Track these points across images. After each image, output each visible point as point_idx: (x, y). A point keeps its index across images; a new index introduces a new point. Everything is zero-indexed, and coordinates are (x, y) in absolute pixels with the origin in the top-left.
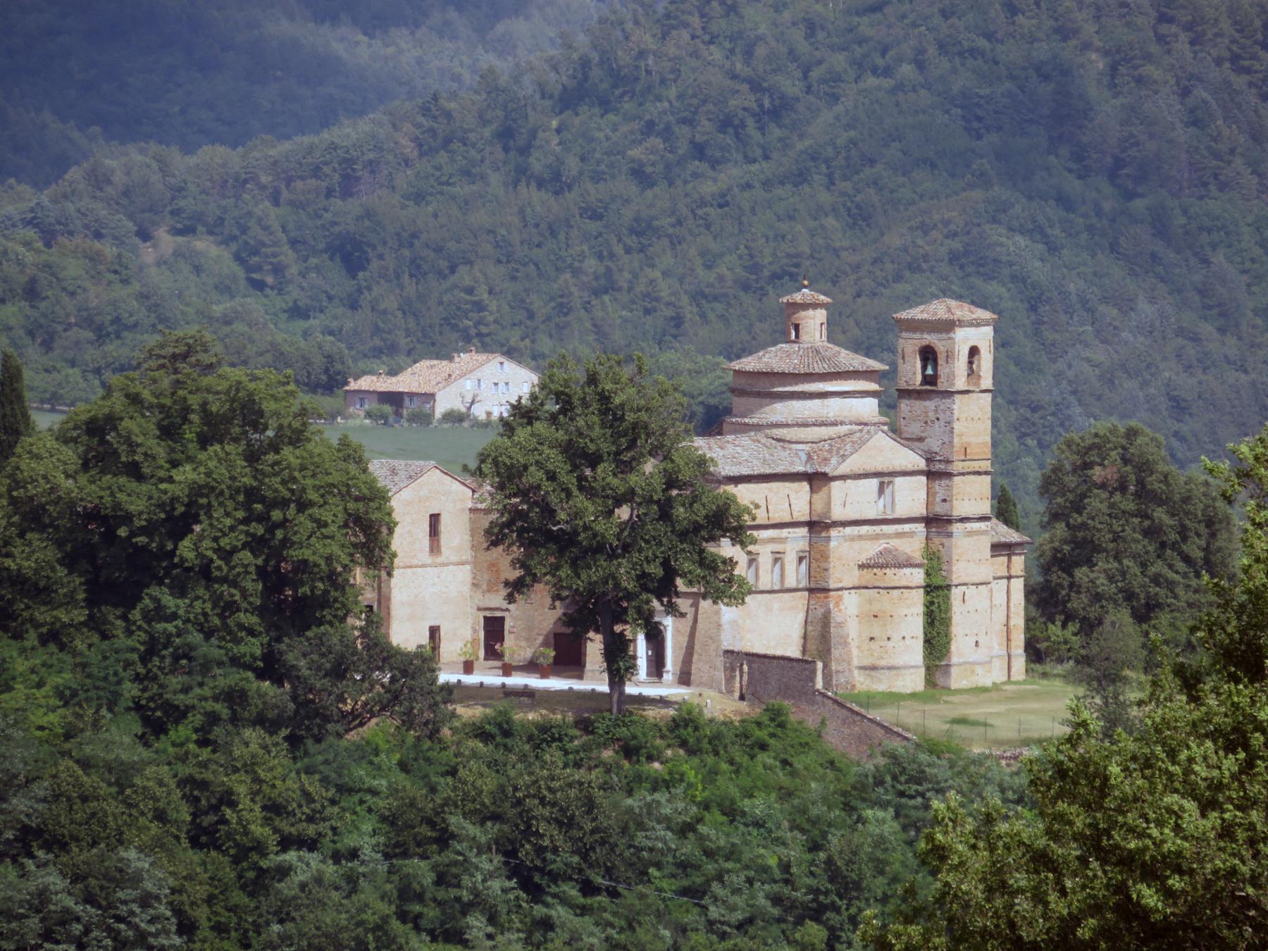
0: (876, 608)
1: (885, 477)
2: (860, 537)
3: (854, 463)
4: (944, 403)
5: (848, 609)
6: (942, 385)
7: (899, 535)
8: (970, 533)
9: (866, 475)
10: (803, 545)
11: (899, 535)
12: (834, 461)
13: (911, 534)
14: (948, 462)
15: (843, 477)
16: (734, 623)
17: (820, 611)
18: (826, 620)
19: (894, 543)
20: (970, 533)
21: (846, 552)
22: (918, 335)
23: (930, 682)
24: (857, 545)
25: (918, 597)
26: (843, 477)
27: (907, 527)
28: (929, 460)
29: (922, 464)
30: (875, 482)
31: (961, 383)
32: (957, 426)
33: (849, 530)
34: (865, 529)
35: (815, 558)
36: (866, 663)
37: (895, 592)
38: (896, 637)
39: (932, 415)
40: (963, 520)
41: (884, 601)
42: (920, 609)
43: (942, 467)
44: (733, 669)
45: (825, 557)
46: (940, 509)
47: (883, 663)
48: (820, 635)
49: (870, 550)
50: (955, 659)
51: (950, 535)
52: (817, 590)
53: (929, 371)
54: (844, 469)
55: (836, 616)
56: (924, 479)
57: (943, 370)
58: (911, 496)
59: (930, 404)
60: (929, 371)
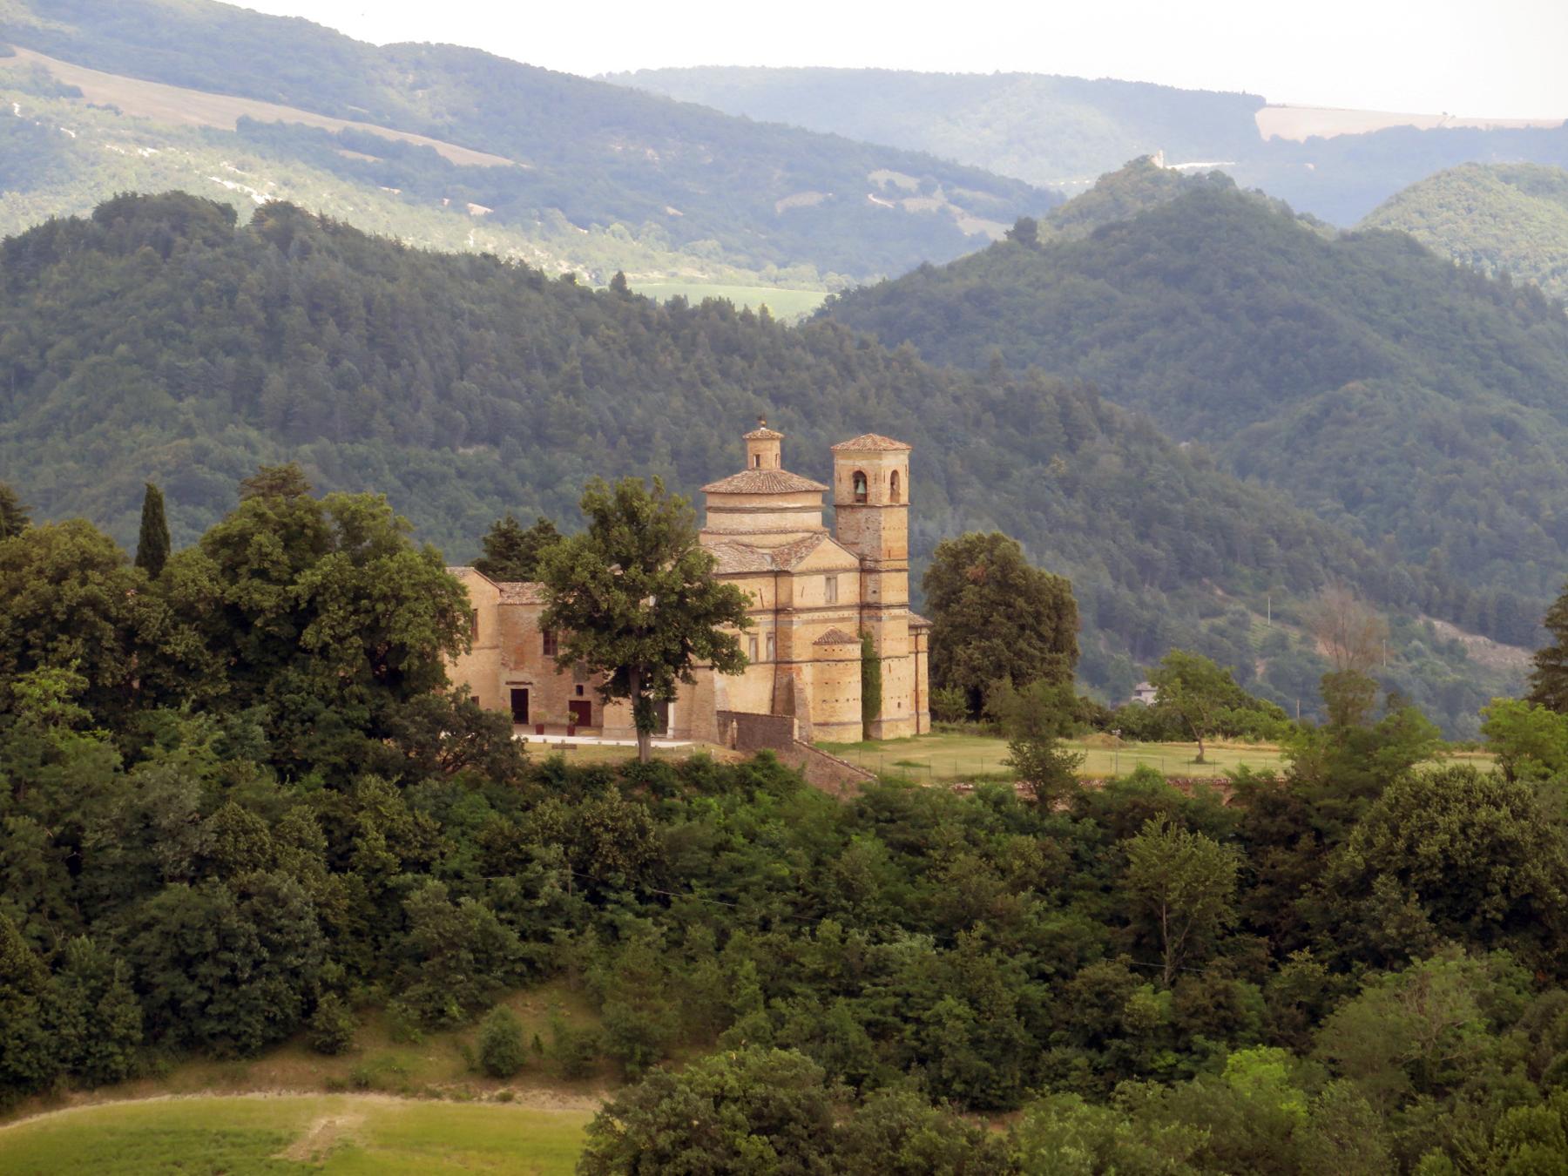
0: (827, 676)
1: (830, 574)
2: (813, 621)
3: (811, 561)
4: (874, 513)
5: (806, 677)
6: (871, 500)
7: (842, 620)
8: (895, 618)
9: (818, 572)
10: (770, 628)
11: (842, 620)
12: (794, 561)
13: (849, 619)
14: (877, 561)
15: (802, 574)
16: (724, 691)
17: (785, 680)
18: (790, 687)
19: (839, 626)
20: (895, 618)
21: (804, 634)
22: (850, 462)
23: (866, 736)
24: (811, 628)
25: (858, 666)
26: (802, 574)
27: (846, 613)
28: (862, 560)
29: (855, 562)
30: (823, 578)
31: (886, 500)
32: (884, 534)
33: (805, 616)
34: (816, 615)
35: (779, 637)
36: (820, 720)
37: (841, 665)
38: (842, 699)
39: (863, 526)
40: (889, 607)
41: (834, 671)
42: (858, 677)
43: (872, 565)
44: (725, 725)
45: (789, 637)
46: (870, 599)
47: (833, 720)
48: (786, 698)
49: (821, 631)
50: (884, 717)
51: (879, 619)
52: (782, 663)
53: (861, 490)
54: (802, 566)
55: (798, 683)
56: (857, 575)
57: (872, 489)
58: (848, 589)
59: (862, 515)
60: (861, 490)
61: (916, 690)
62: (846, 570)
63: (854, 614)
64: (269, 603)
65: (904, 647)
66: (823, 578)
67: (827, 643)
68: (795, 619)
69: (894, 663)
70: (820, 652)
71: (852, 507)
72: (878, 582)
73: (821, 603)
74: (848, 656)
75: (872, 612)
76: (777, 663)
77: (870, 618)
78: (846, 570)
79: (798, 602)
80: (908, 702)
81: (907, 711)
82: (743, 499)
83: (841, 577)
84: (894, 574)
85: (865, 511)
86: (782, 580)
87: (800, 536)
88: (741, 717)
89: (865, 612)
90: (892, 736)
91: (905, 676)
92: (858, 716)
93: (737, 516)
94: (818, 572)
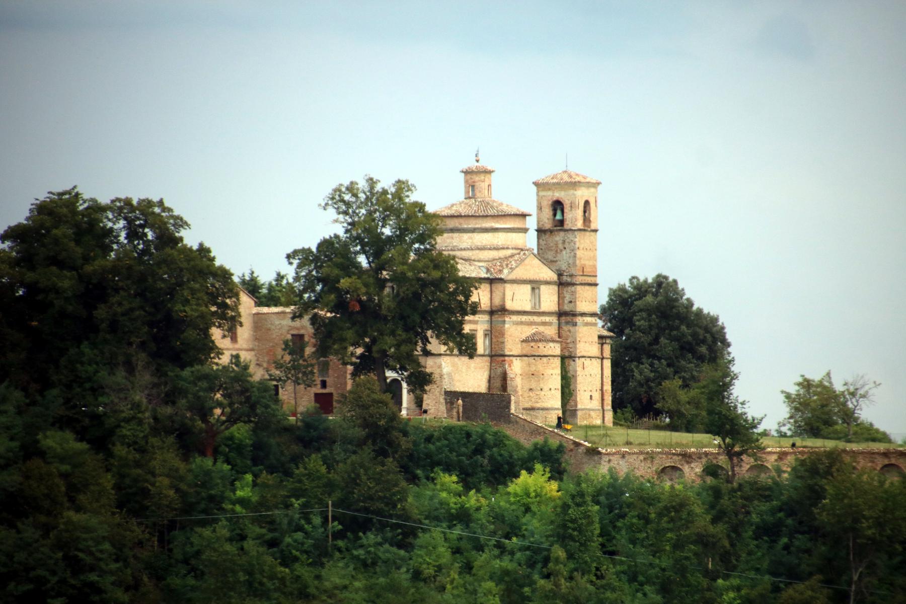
0: (533, 369)
1: (535, 285)
2: (522, 323)
4: (570, 236)
5: (516, 369)
6: (568, 225)
7: (544, 324)
8: (587, 324)
10: (486, 326)
11: (544, 324)
12: (506, 271)
13: (550, 324)
14: (571, 276)
16: (449, 374)
17: (500, 370)
19: (541, 329)
20: (587, 324)
21: (515, 334)
22: (550, 193)
24: (519, 328)
25: (558, 362)
27: (547, 319)
28: (560, 275)
29: (555, 277)
31: (580, 224)
32: (579, 253)
33: (515, 318)
34: (524, 318)
35: (495, 334)
36: (527, 405)
37: (545, 359)
38: (546, 388)
39: (561, 246)
40: (583, 314)
42: (558, 371)
43: (569, 280)
44: (452, 403)
45: (502, 334)
46: (567, 308)
47: (538, 405)
48: (500, 383)
49: (528, 331)
50: (579, 406)
51: (575, 324)
52: (497, 356)
53: (559, 217)
54: (512, 276)
55: (510, 374)
56: (556, 288)
57: (568, 216)
58: (549, 299)
59: (559, 237)
60: (559, 217)
61: (602, 390)
62: (547, 283)
63: (554, 320)
64: (66, 284)
65: (594, 350)
67: (533, 340)
68: (507, 319)
69: (587, 362)
70: (527, 349)
71: (551, 231)
72: (573, 293)
73: (528, 308)
75: (569, 318)
77: (567, 323)
78: (547, 283)
79: (509, 305)
80: (597, 395)
81: (596, 404)
82: (461, 220)
83: (543, 287)
84: (587, 287)
85: (562, 234)
86: (498, 287)
88: (465, 395)
89: (563, 319)
90: (585, 423)
91: (594, 379)
92: (558, 404)
93: (456, 235)
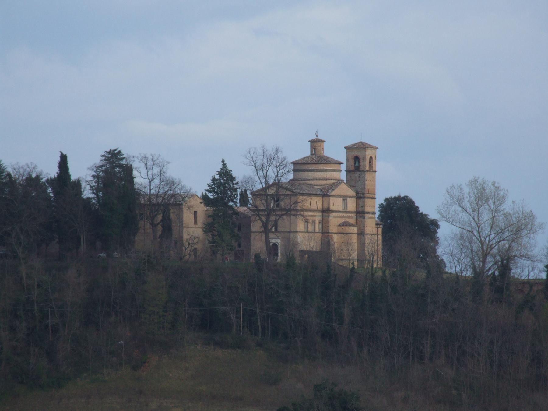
1: (345, 198)
2: (338, 217)
6: (362, 168)
7: (349, 217)
9: (340, 196)
10: (320, 218)
11: (349, 217)
12: (330, 191)
14: (363, 194)
21: (334, 221)
27: (350, 215)
28: (357, 192)
29: (354, 194)
30: (341, 199)
31: (367, 168)
32: (367, 183)
33: (334, 214)
34: (339, 214)
40: (369, 213)
46: (360, 210)
49: (341, 221)
51: (364, 218)
53: (357, 165)
54: (333, 193)
56: (355, 199)
57: (362, 164)
58: (352, 205)
60: (357, 165)
62: (351, 197)
63: (354, 215)
66: (341, 199)
67: (343, 225)
70: (341, 229)
72: (364, 202)
74: (352, 232)
75: (361, 215)
76: (323, 233)
77: (361, 217)
78: (351, 197)
79: (332, 208)
82: (309, 166)
84: (370, 200)
86: (326, 199)
87: (332, 181)
89: (358, 215)
94: (340, 196)
